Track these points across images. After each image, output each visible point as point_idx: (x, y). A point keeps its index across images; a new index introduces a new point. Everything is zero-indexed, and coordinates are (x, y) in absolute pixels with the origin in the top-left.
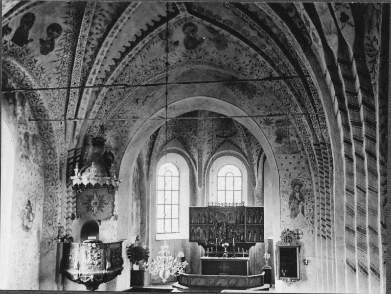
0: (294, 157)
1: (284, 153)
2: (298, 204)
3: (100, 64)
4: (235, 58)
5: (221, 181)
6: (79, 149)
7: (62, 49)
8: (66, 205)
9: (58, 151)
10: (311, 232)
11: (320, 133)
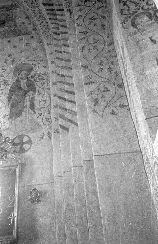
10: (46, 137)
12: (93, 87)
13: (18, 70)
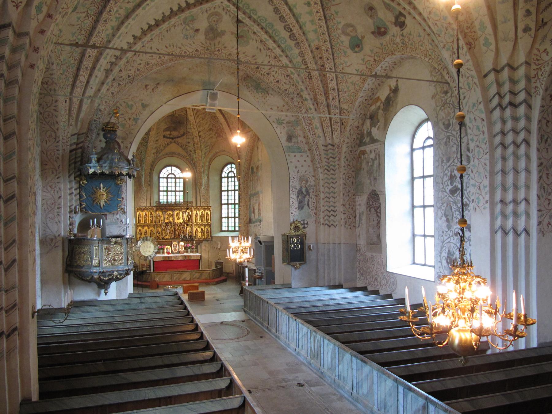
0: (302, 156)
1: (294, 152)
2: (305, 198)
3: (121, 38)
4: (253, 56)
5: (163, 182)
6: (83, 134)
7: (84, 12)
8: (68, 197)
9: (61, 134)
11: (331, 135)
12: (346, 216)
13: (301, 179)
